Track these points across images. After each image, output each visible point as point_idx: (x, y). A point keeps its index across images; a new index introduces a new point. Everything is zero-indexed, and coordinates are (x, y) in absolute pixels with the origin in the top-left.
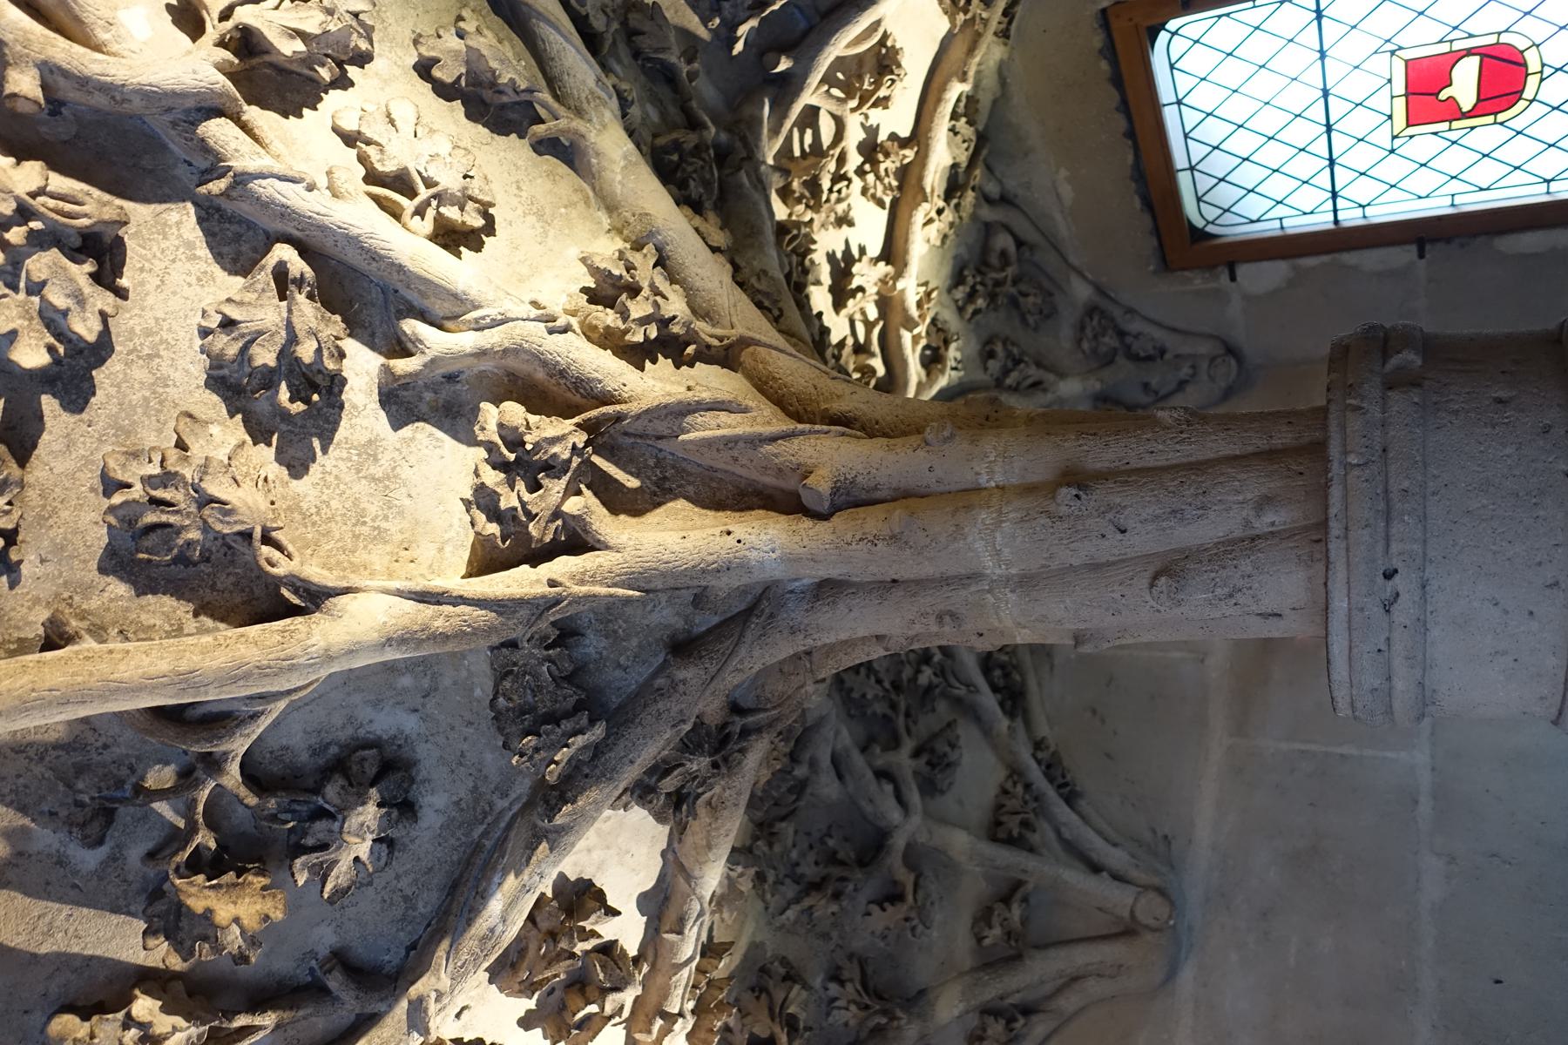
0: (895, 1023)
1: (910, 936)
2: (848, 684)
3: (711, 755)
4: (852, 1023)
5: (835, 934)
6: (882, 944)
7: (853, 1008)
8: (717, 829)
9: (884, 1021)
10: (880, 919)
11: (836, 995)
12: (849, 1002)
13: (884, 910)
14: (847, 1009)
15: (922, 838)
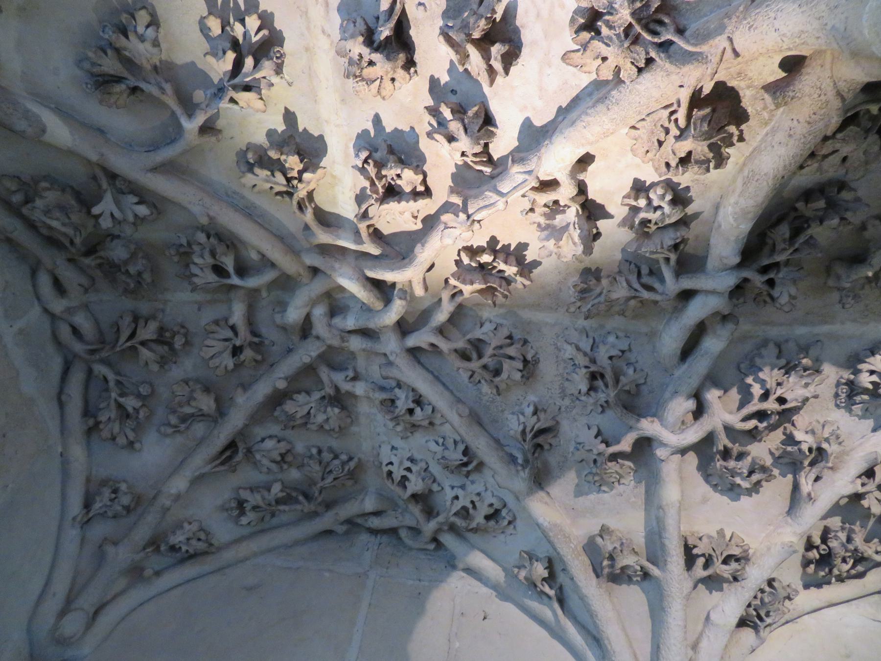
0: (520, 468)
1: (586, 473)
2: (764, 352)
3: (633, 14)
4: (512, 432)
5: (567, 402)
6: (572, 449)
7: (521, 428)
8: (587, 114)
9: (520, 461)
10: (587, 436)
11: (526, 415)
12: (524, 423)
13: (596, 437)
14: (519, 425)
15: (660, 453)
